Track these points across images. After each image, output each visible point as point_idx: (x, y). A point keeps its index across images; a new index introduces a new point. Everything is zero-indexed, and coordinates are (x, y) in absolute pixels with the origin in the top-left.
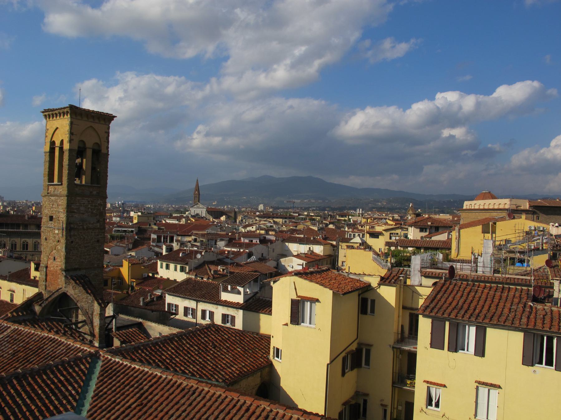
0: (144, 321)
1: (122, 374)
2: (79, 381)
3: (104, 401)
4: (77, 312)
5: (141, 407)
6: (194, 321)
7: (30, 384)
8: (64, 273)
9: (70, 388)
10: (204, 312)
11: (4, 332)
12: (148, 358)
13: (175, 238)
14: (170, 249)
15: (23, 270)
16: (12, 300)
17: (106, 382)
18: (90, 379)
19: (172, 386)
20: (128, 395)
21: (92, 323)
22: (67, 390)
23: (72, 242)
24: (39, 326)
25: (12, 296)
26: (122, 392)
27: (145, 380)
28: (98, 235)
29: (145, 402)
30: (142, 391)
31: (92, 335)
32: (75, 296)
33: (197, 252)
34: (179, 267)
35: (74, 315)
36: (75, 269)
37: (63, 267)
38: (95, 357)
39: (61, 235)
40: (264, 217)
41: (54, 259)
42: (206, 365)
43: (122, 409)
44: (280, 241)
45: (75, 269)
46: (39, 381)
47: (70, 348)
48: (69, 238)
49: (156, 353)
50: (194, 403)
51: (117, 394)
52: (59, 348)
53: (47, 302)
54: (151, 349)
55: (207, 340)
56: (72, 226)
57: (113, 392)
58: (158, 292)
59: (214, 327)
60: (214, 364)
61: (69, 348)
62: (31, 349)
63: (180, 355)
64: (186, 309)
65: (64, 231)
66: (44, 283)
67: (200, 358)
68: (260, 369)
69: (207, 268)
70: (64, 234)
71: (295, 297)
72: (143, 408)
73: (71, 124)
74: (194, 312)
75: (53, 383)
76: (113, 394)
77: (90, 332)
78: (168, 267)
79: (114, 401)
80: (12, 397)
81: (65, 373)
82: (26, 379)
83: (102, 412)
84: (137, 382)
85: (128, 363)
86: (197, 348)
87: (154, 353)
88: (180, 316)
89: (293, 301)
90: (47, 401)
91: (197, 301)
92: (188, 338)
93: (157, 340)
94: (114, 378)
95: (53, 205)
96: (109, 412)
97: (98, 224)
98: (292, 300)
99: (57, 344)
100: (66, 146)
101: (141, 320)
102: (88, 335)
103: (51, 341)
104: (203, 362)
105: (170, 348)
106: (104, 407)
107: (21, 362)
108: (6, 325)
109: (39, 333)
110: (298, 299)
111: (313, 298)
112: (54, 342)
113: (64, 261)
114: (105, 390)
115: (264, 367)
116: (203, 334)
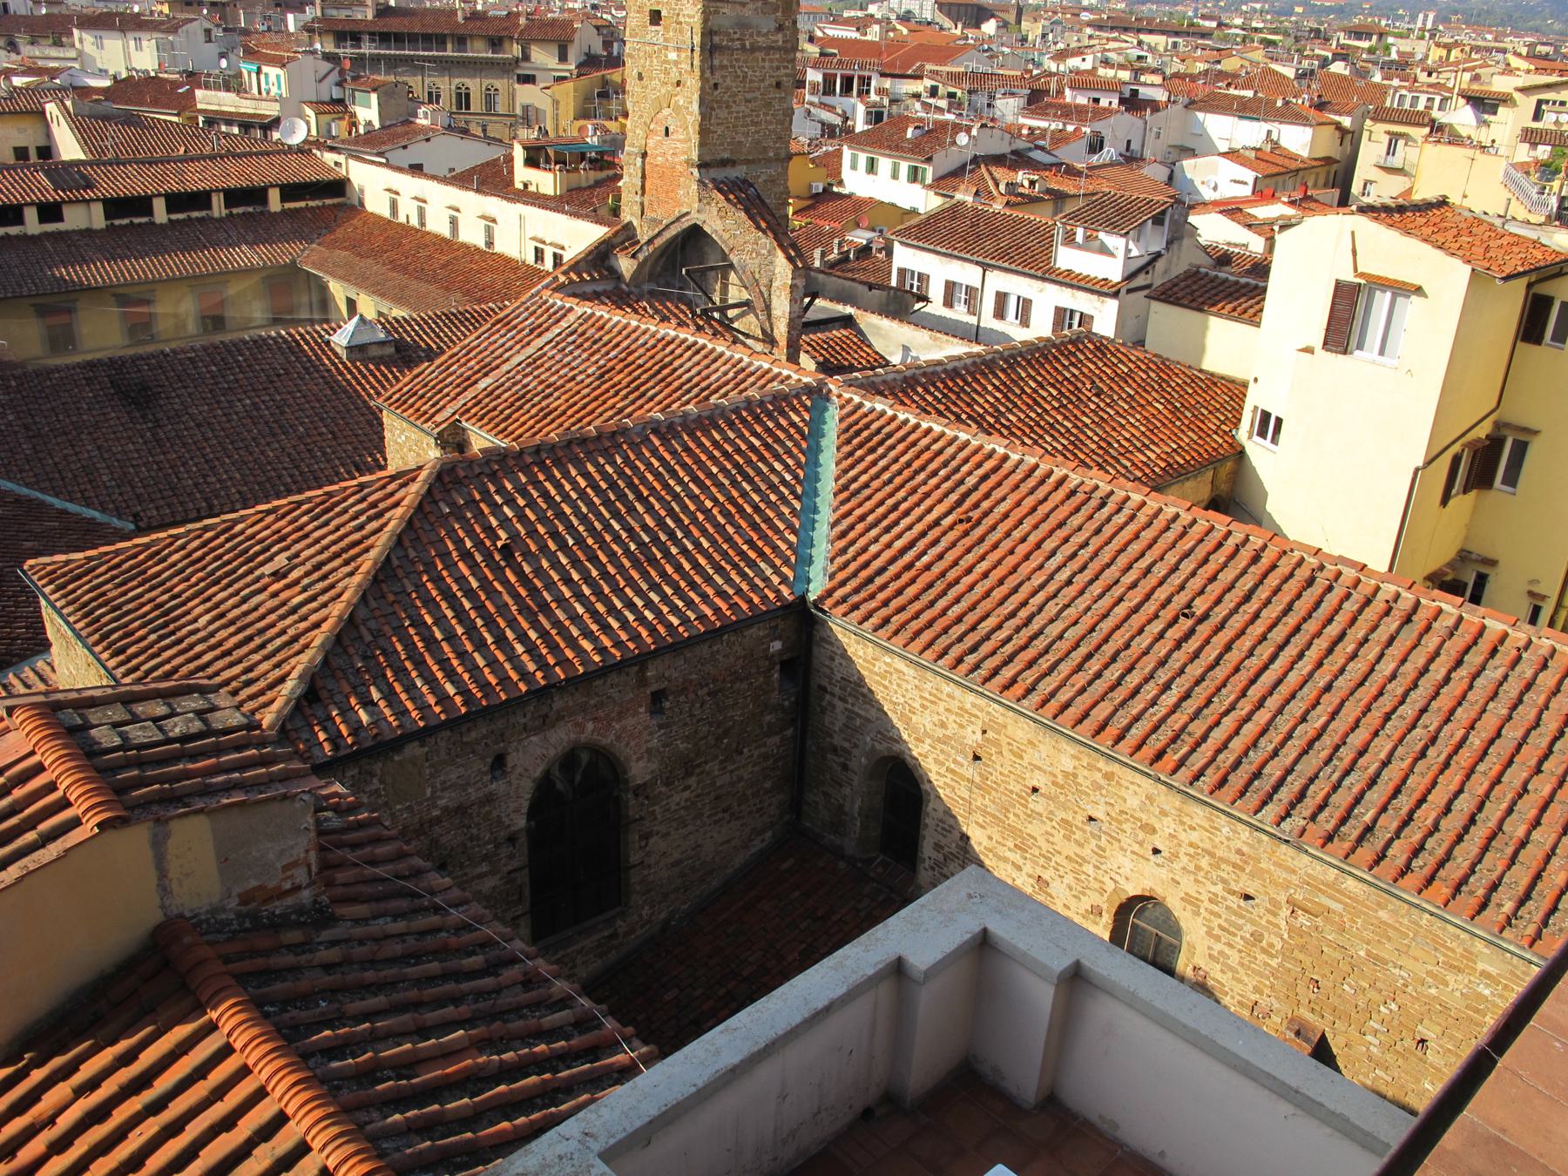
0: (859, 312)
1: (900, 441)
2: (795, 451)
3: (868, 505)
4: (725, 277)
5: (965, 526)
6: (973, 320)
7: (687, 449)
8: (695, 171)
9: (777, 466)
10: (1001, 298)
11: (558, 321)
12: (941, 407)
13: (873, 83)
14: (876, 116)
15: (488, 164)
16: (490, 244)
17: (862, 459)
18: (814, 451)
19: (1042, 482)
20: (927, 495)
21: (768, 308)
22: (773, 470)
23: (716, 85)
24: (636, 312)
25: (489, 232)
26: (908, 486)
27: (966, 461)
28: (778, 68)
29: (975, 514)
30: (962, 489)
31: (769, 339)
32: (726, 236)
33: (957, 128)
34: (904, 167)
35: (718, 287)
36: (724, 163)
37: (695, 156)
38: (818, 394)
39: (686, 66)
41: (667, 134)
42: (1082, 437)
43: (919, 528)
44: (1179, 107)
45: (724, 163)
46: (708, 444)
47: (743, 370)
48: (708, 74)
49: (959, 397)
50: (1108, 530)
51: (897, 489)
52: (714, 367)
53: (651, 248)
54: (946, 386)
55: (1076, 372)
56: (716, 39)
57: (886, 484)
58: (860, 237)
59: (1090, 341)
60: (1101, 439)
61: (742, 373)
62: (640, 366)
63: (1016, 405)
64: (950, 287)
65: (697, 54)
66: (638, 199)
67: (1066, 418)
68: (1214, 461)
69: (986, 175)
70: (697, 62)
71: (1349, 277)
72: (973, 528)
74: (972, 297)
75: (738, 451)
76: (888, 489)
77: (763, 330)
78: (872, 167)
79: (895, 507)
80: (658, 476)
81: (759, 429)
82: (677, 436)
83: (868, 530)
84: (945, 464)
85: (911, 417)
86: (1055, 393)
87: (953, 397)
88: (936, 307)
89: (1339, 286)
90: (735, 494)
91: (986, 267)
92: (1029, 363)
93: (956, 364)
94: (881, 450)
96: (887, 530)
97: (780, 36)
98: (1338, 283)
99: (706, 357)
101: (849, 310)
102: (757, 339)
103: (689, 348)
104: (1074, 431)
105: (990, 388)
106: (870, 519)
107: (626, 397)
108: (559, 303)
109: (653, 328)
110: (1358, 280)
111: (1404, 283)
112: (698, 352)
113: (695, 138)
114: (864, 478)
115: (1225, 458)
116: (1067, 358)
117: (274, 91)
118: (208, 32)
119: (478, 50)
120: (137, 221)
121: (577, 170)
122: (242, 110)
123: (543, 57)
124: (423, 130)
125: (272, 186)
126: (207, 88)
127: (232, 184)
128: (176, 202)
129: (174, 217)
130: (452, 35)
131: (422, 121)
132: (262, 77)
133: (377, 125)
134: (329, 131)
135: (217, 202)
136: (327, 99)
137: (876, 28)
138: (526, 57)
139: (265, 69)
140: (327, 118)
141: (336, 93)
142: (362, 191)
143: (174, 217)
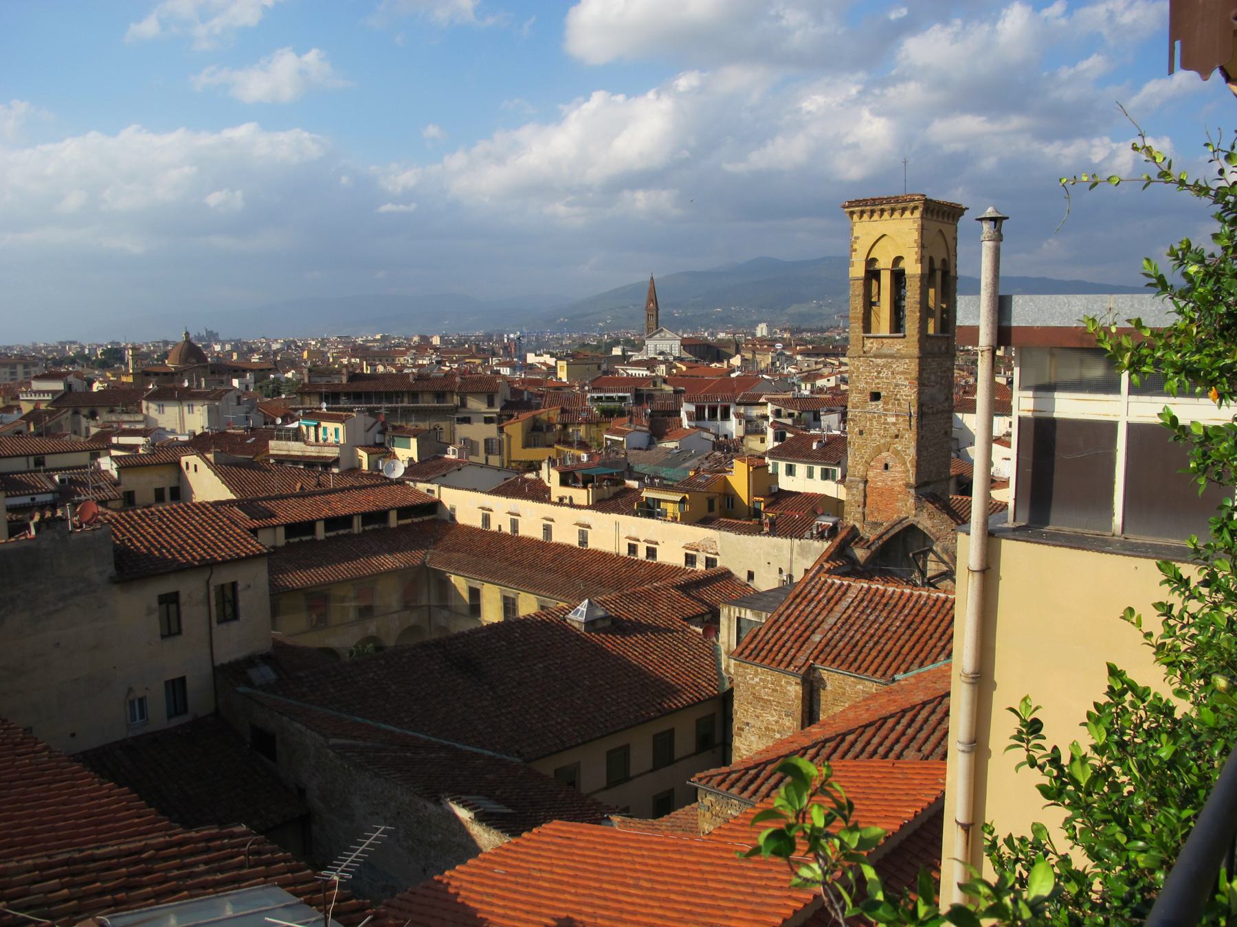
13: (732, 410)
16: (583, 542)
32: (934, 530)
34: (817, 470)
37: (912, 480)
40: (818, 355)
53: (880, 542)
73: (923, 229)
95: (879, 373)
100: (913, 268)
117: (332, 439)
118: (239, 397)
119: (427, 402)
120: (304, 538)
121: (600, 487)
123: (476, 404)
124: (451, 463)
125: (392, 509)
126: (279, 438)
127: (366, 508)
128: (331, 523)
129: (328, 534)
131: (450, 456)
132: (321, 431)
133: (416, 460)
134: (377, 466)
135: (357, 522)
137: (663, 367)
138: (464, 405)
139: (323, 424)
140: (375, 457)
141: (378, 439)
142: (453, 509)
143: (328, 534)
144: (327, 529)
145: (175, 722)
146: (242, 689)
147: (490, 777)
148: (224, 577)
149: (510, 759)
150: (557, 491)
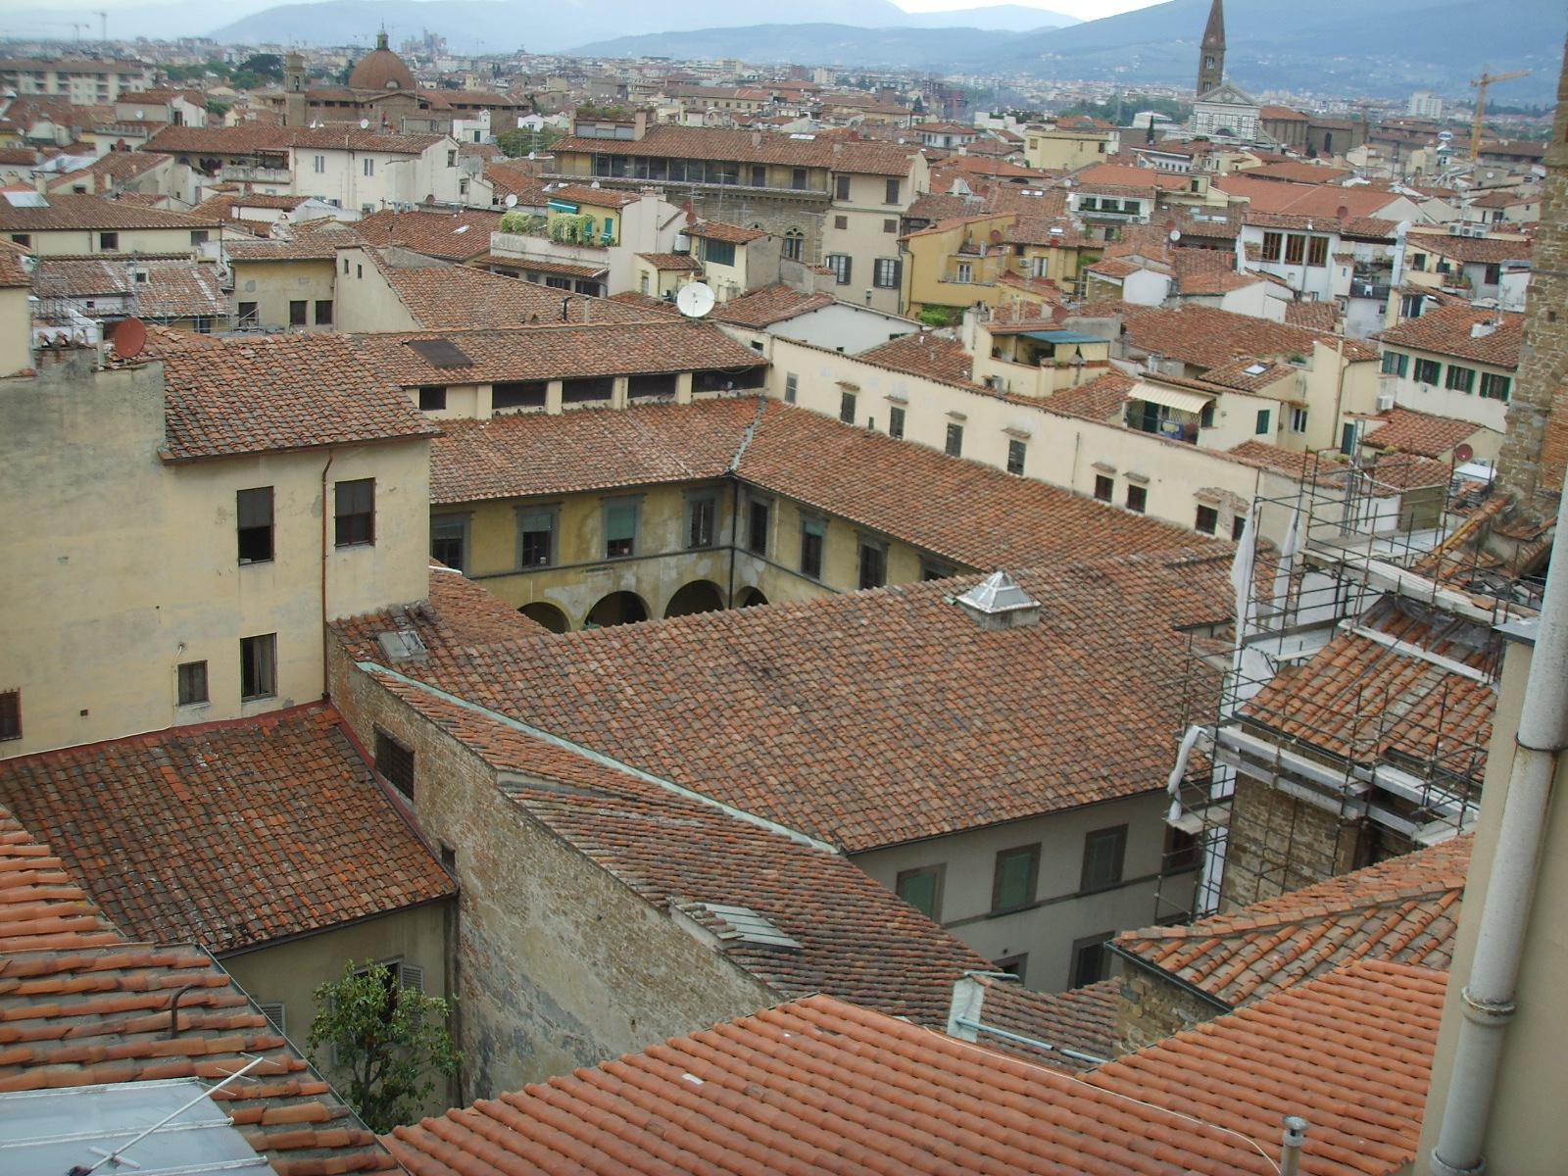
40: (1517, 158)
120: (525, 410)
122: (555, 261)
129: (569, 406)
130: (748, 164)
136: (668, 251)
144: (567, 397)
145: (258, 707)
146: (365, 666)
147: (772, 874)
148: (352, 469)
149: (816, 845)
150: (984, 366)
